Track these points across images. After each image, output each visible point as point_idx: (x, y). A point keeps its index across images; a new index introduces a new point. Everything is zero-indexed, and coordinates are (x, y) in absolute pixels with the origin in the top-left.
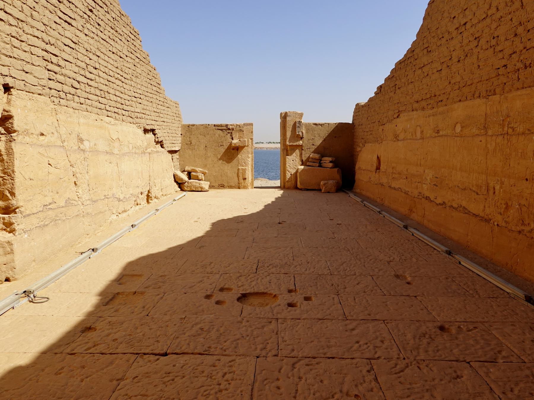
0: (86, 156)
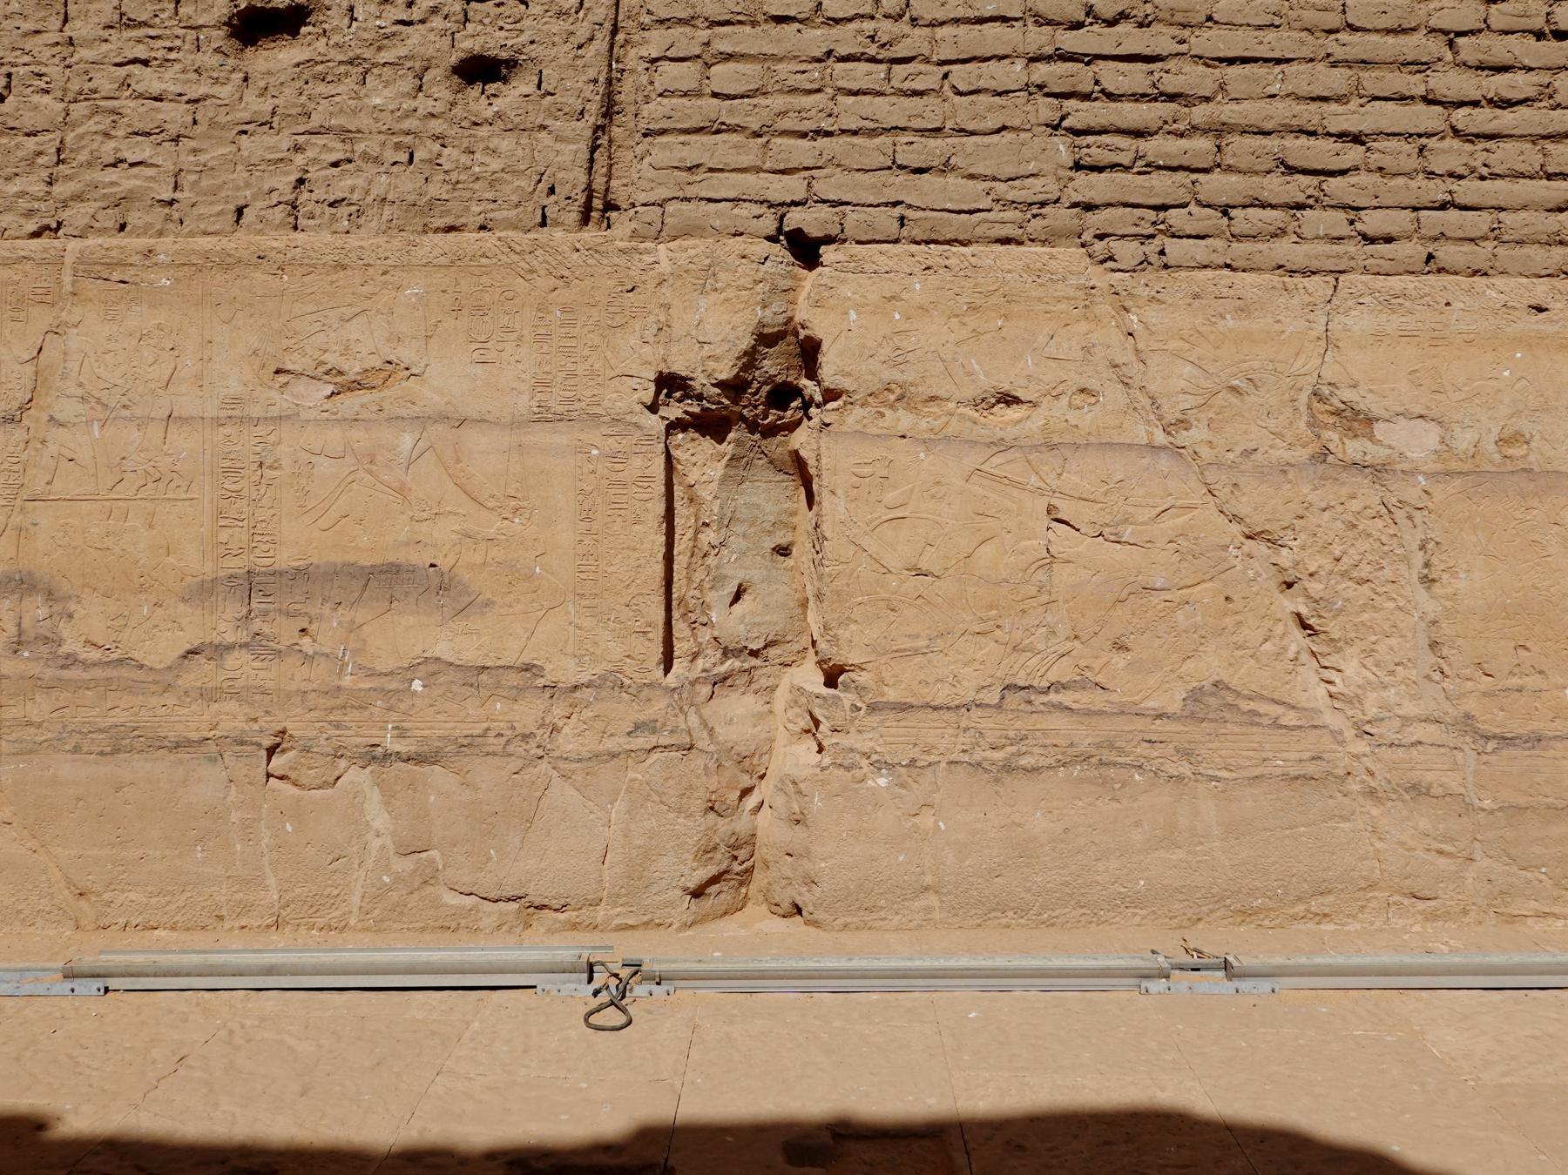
0: (1412, 494)
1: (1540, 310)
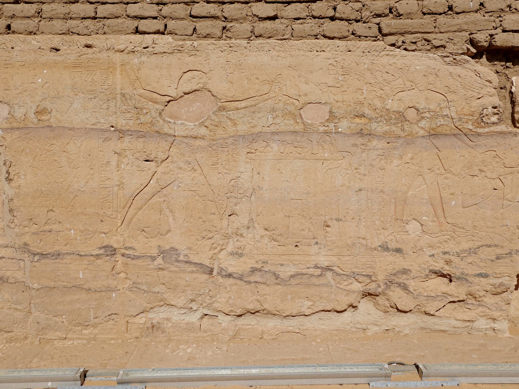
1: (58, 50)
